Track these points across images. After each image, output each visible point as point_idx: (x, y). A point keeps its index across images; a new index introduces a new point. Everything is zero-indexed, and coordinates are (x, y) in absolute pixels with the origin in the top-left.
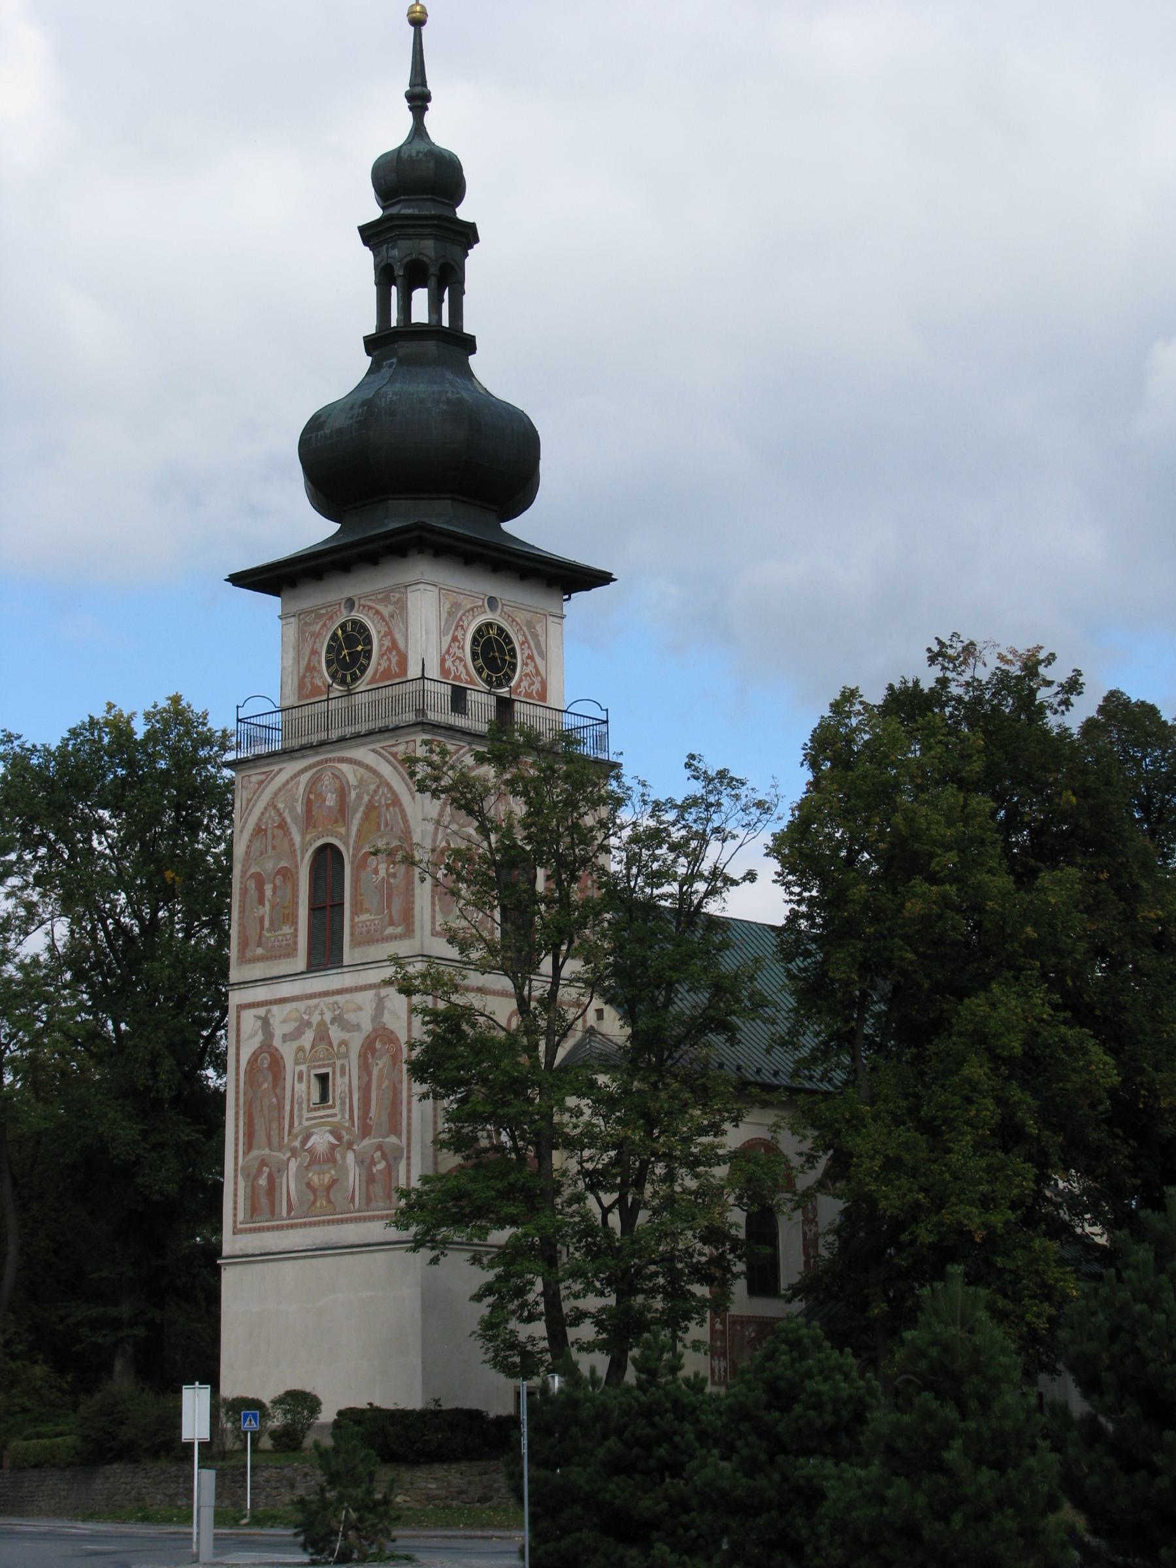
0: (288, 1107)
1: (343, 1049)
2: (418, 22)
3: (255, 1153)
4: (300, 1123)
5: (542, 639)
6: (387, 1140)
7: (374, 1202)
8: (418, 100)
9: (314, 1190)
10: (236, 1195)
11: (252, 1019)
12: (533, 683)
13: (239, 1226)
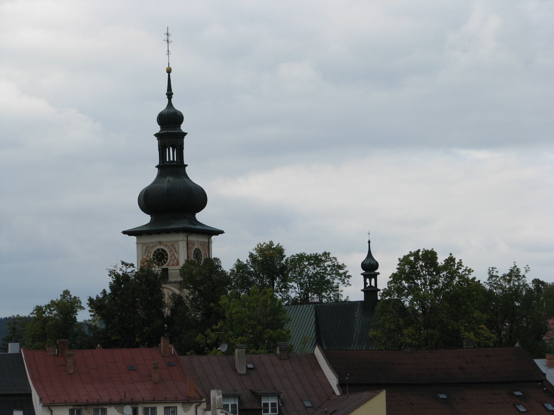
2: (169, 71)
5: (177, 248)
8: (170, 95)
12: (174, 261)
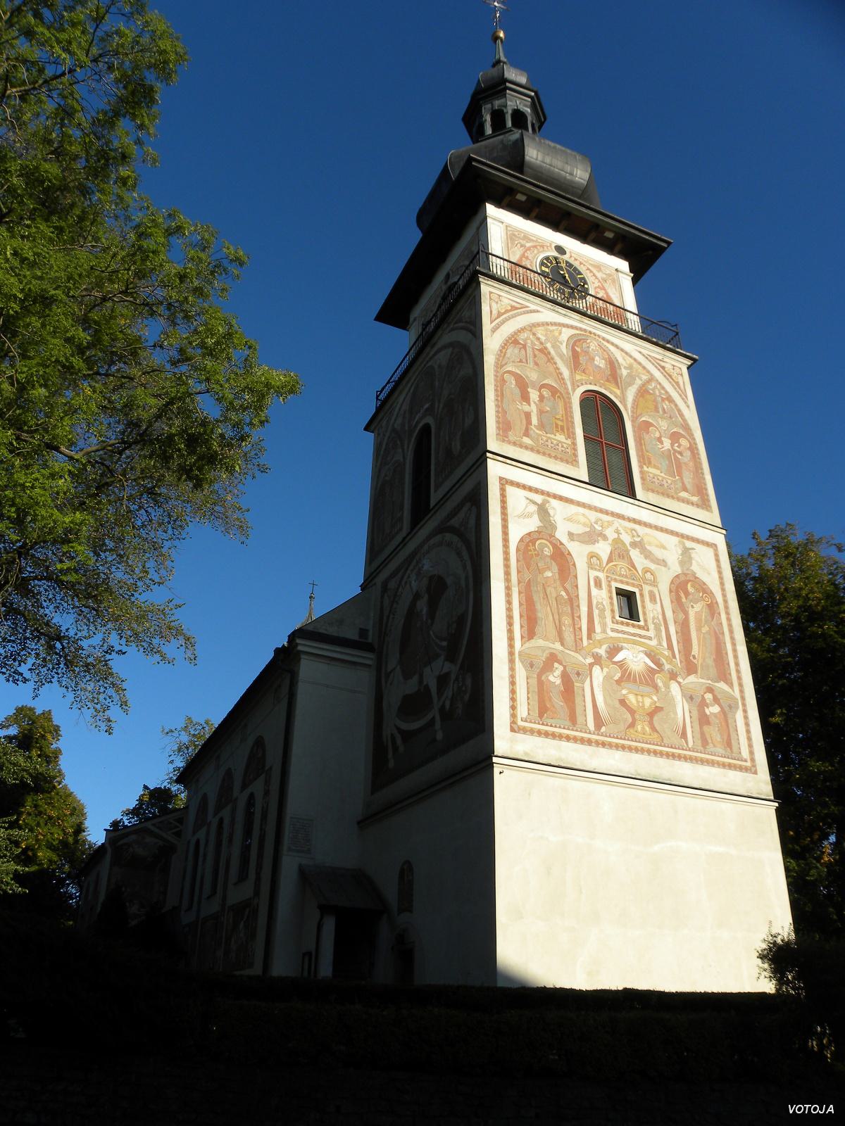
0: (584, 609)
1: (648, 576)
3: (538, 642)
4: (604, 631)
6: (716, 684)
7: (711, 745)
9: (632, 712)
10: (513, 683)
11: (524, 502)
13: (520, 723)
